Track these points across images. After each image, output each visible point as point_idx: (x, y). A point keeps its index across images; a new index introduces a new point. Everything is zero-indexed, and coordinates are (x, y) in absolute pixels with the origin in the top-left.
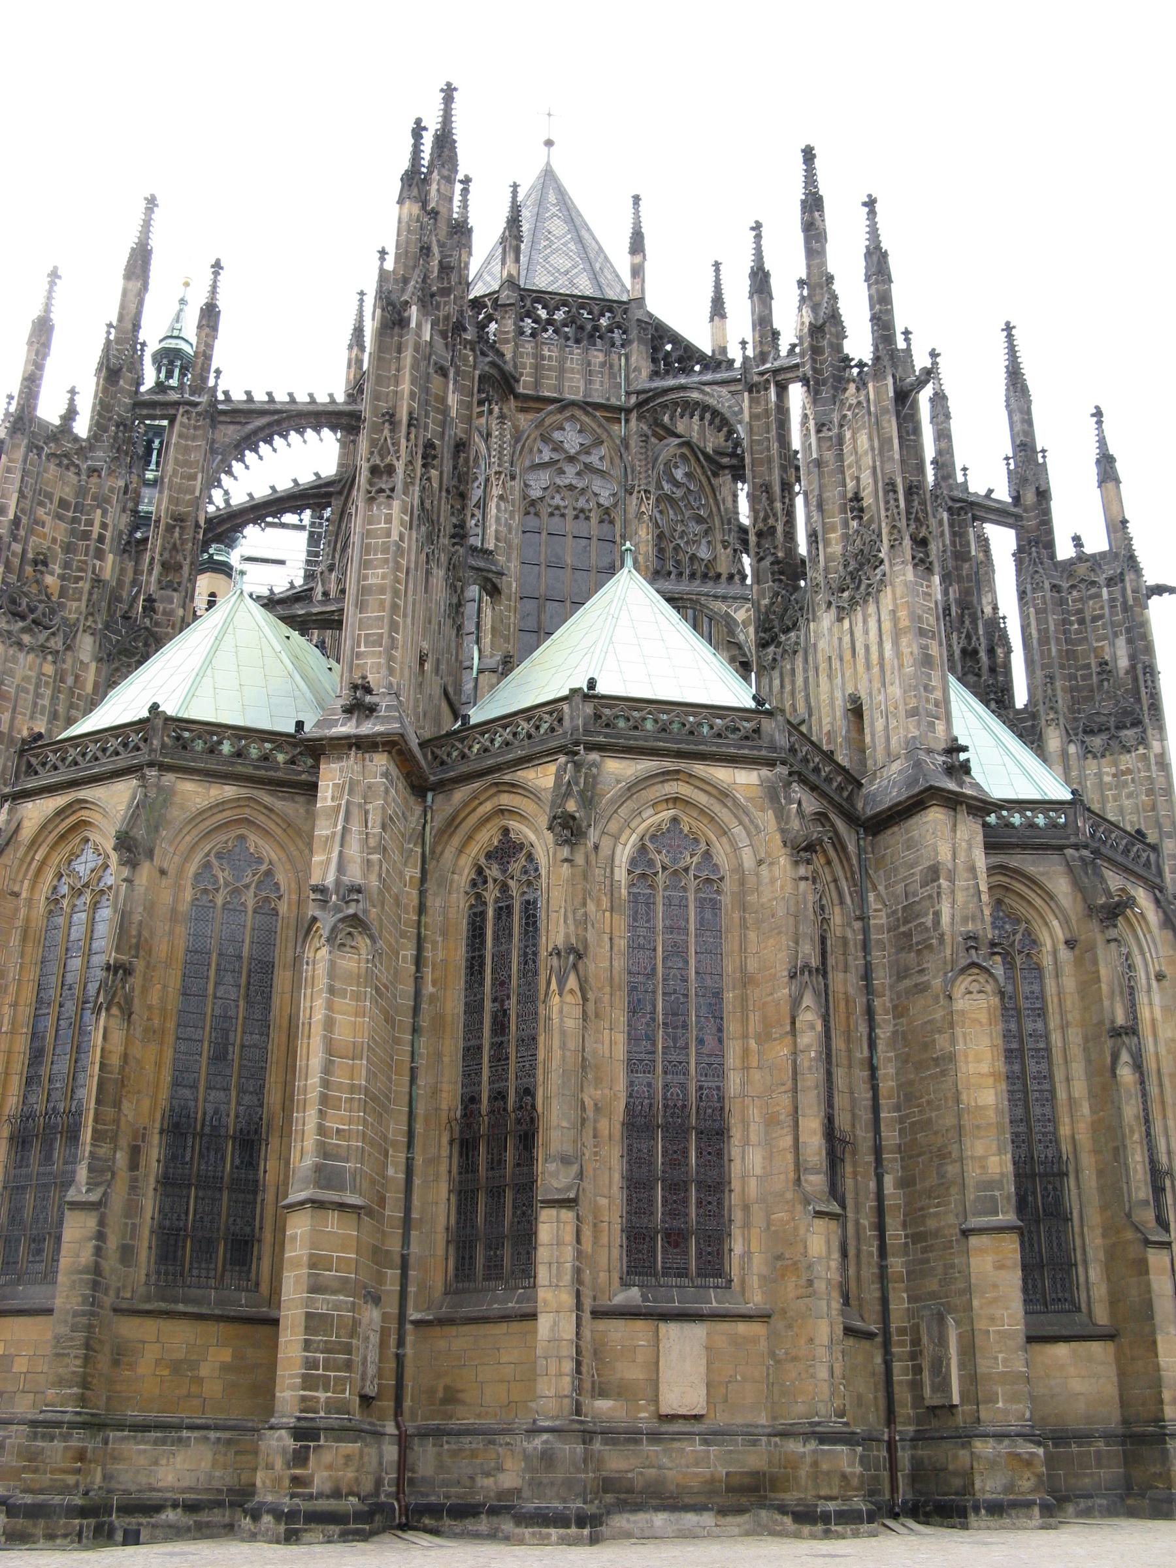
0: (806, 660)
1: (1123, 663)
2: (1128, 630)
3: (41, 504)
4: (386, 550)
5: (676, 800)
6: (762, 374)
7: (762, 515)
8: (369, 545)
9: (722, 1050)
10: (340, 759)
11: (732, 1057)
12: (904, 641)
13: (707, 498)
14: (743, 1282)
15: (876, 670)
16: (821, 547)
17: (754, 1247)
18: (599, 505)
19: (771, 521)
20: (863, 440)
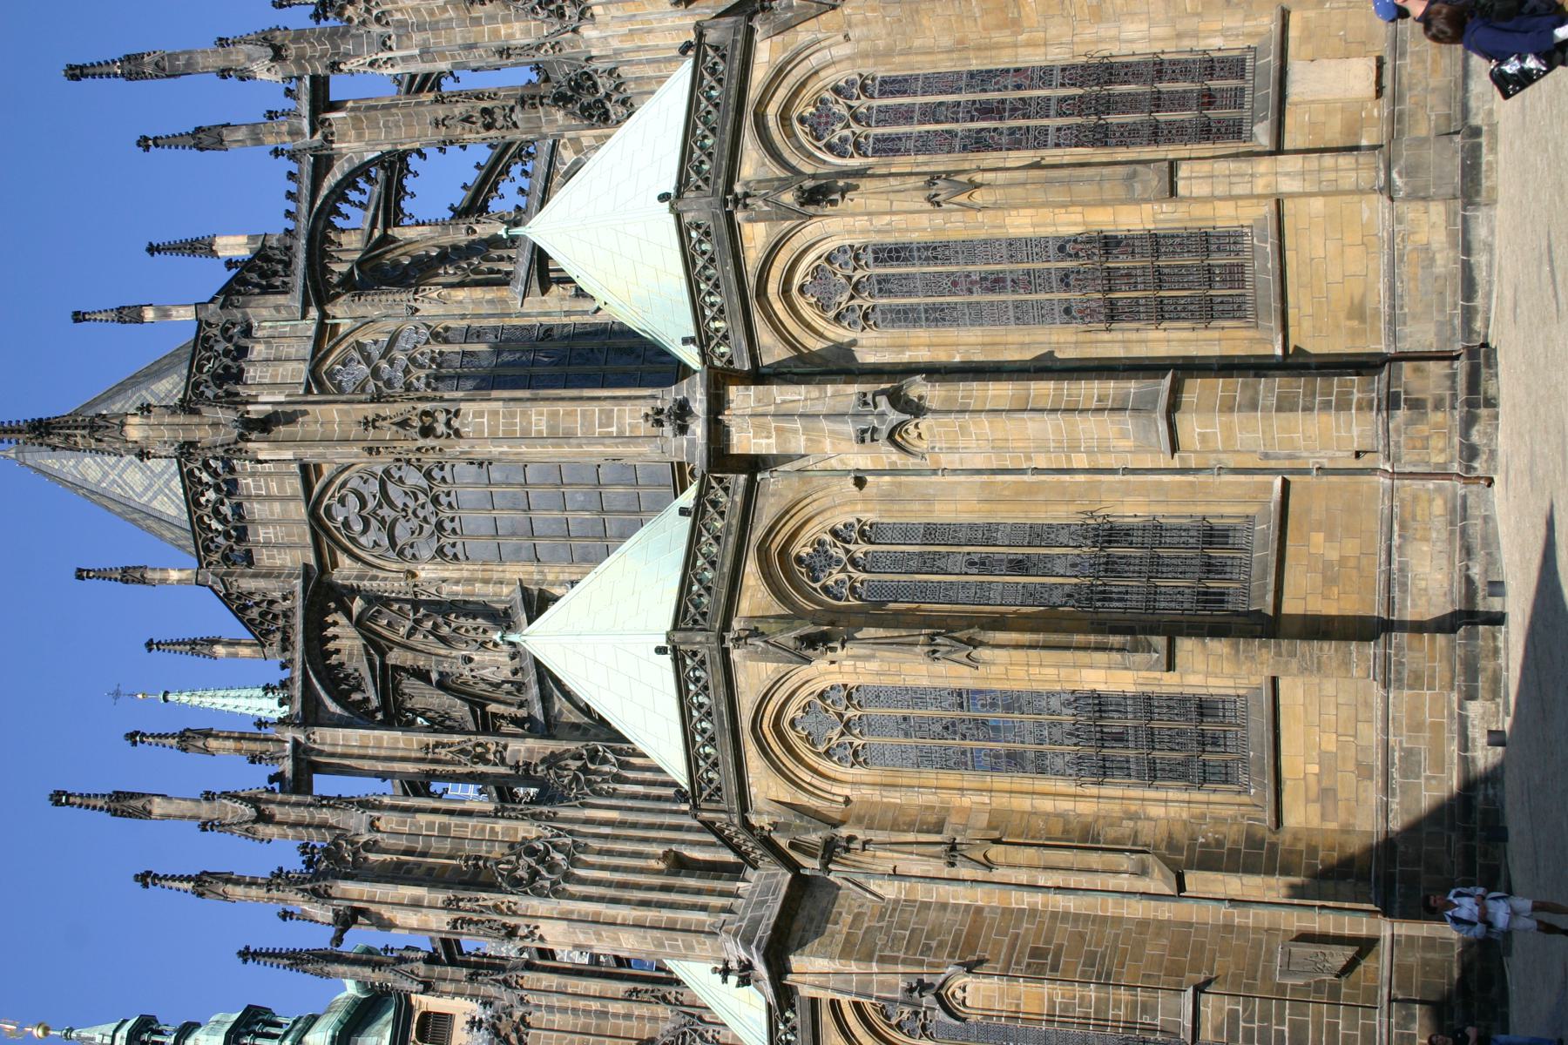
5: (784, 117)
6: (313, 132)
9: (1026, 69)
10: (728, 433)
11: (1032, 58)
14: (1250, 35)
17: (1217, 26)
18: (427, 342)
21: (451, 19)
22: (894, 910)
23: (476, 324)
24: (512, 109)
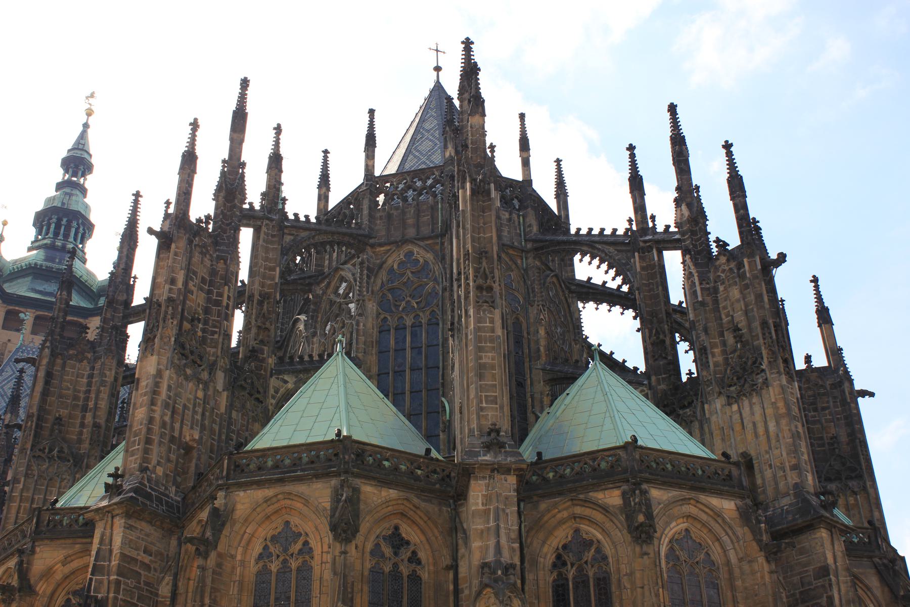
0: (701, 428)
1: (844, 438)
2: (846, 418)
3: (192, 279)
4: (492, 340)
5: (689, 516)
6: (645, 242)
7: (654, 331)
8: (480, 337)
12: (784, 422)
13: (565, 311)
15: (763, 438)
16: (710, 356)
19: (661, 337)
20: (735, 293)
21: (721, 319)
22: (151, 593)
23: (525, 341)
24: (665, 358)
